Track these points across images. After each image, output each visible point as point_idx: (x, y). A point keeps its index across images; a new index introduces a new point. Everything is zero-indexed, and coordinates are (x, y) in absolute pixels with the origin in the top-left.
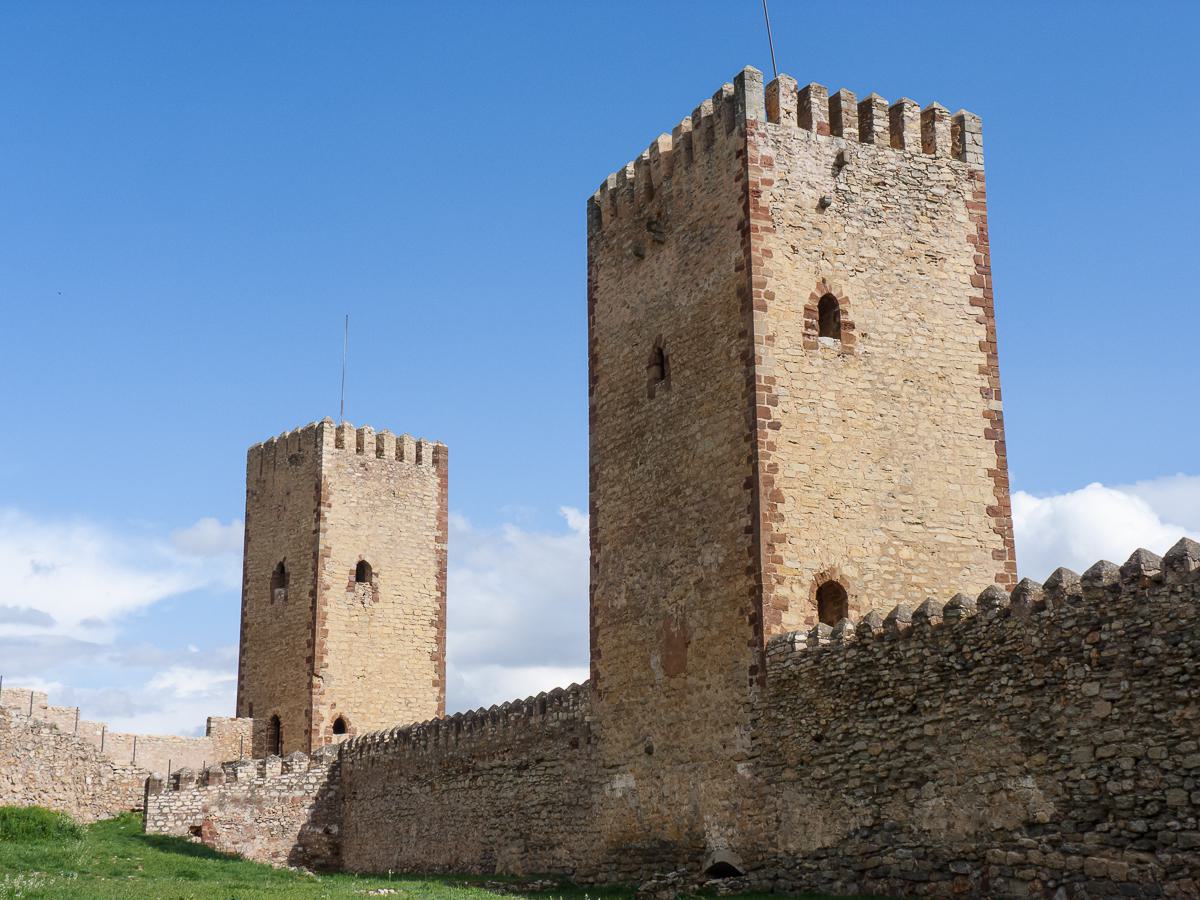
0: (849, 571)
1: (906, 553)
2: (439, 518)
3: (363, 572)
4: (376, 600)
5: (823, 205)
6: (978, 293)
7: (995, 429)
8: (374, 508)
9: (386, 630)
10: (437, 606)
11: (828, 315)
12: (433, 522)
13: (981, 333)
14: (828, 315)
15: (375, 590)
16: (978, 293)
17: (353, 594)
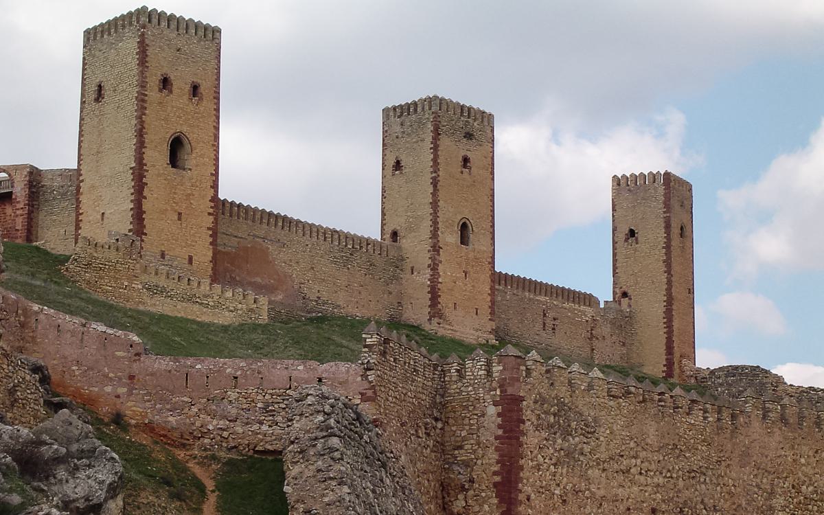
0: (399, 228)
1: (411, 220)
2: (665, 203)
3: (632, 233)
4: (637, 243)
5: (397, 137)
6: (432, 146)
7: (435, 183)
8: (634, 207)
9: (642, 255)
10: (665, 240)
11: (398, 165)
12: (662, 206)
13: (432, 156)
14: (398, 165)
15: (637, 239)
16: (432, 146)
17: (626, 243)
